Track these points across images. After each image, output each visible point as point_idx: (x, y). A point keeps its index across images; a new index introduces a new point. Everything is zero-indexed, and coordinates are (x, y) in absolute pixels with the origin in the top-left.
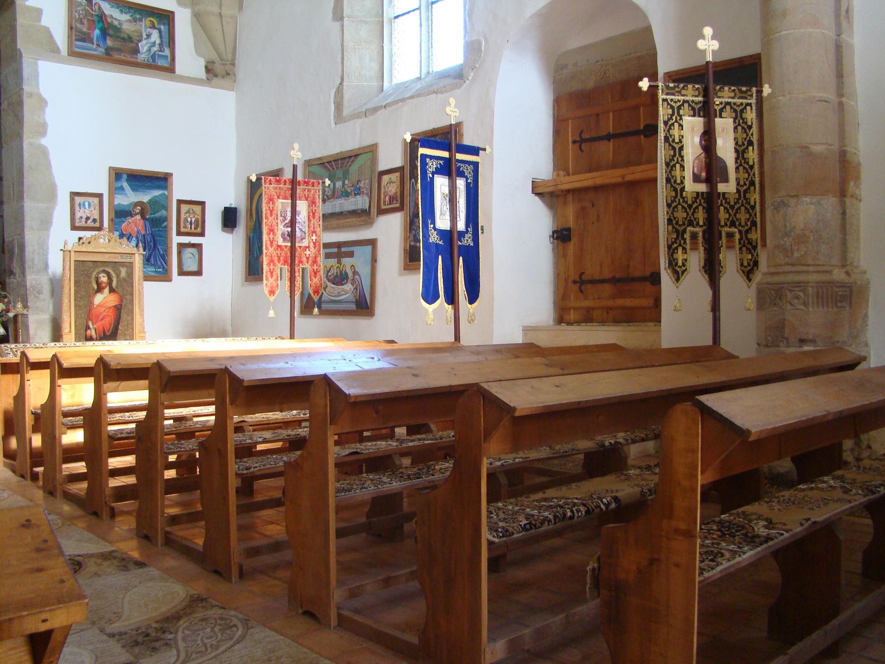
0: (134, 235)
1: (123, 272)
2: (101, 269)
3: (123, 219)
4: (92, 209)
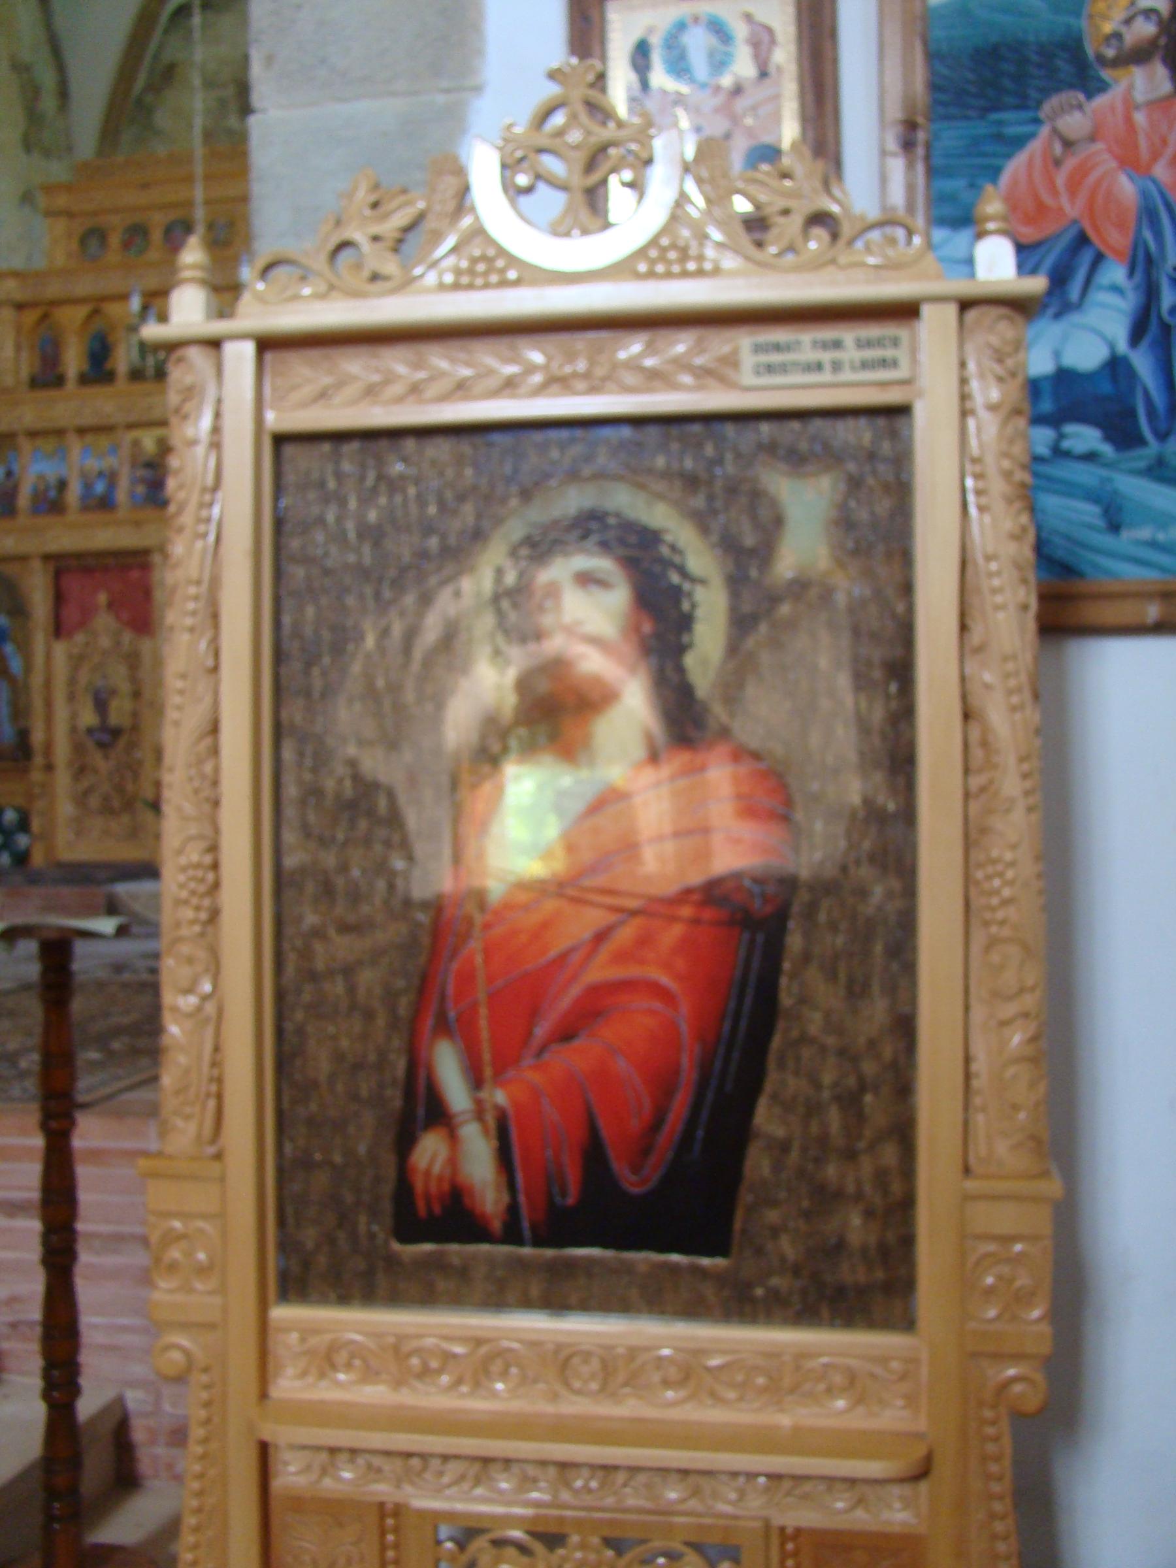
0: (1116, 238)
1: (806, 507)
2: (573, 501)
3: (1012, 121)
4: (743, 66)
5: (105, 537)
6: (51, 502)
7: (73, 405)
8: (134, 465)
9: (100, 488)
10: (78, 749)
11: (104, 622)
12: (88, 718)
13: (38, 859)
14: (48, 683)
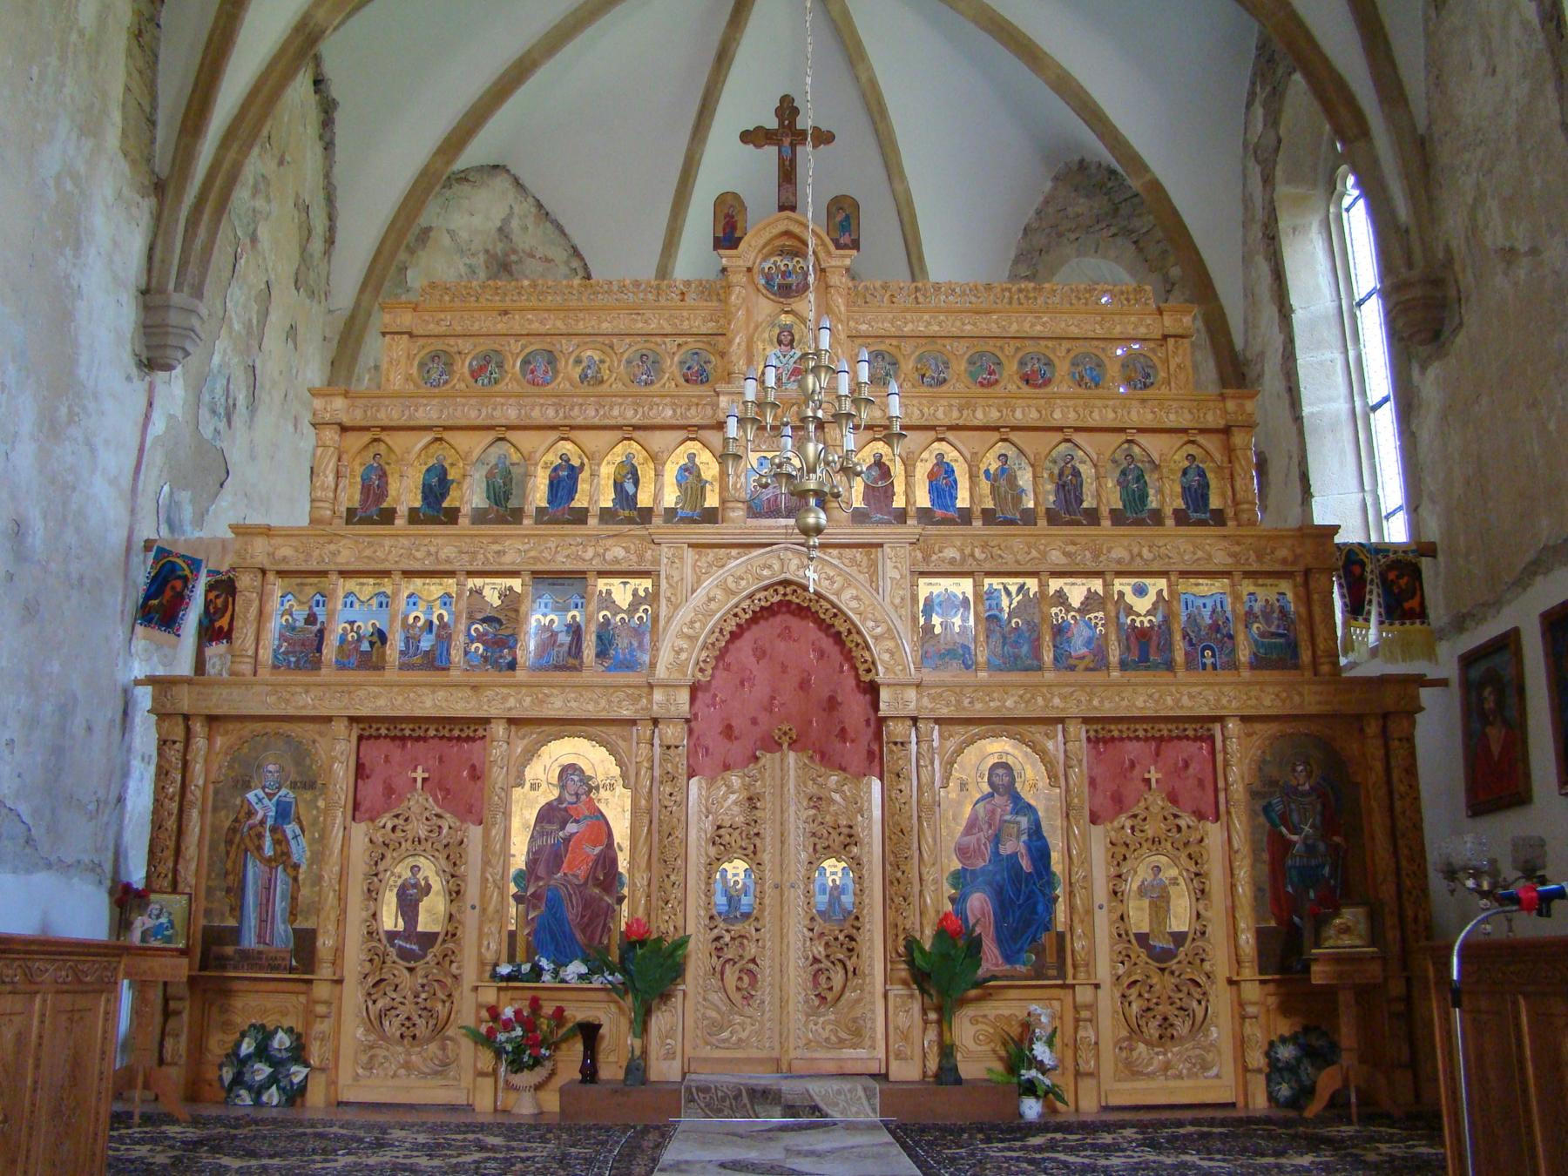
5: (432, 701)
6: (368, 654)
7: (396, 545)
8: (472, 620)
9: (426, 643)
10: (376, 959)
11: (419, 802)
12: (390, 919)
13: (316, 1096)
14: (342, 876)
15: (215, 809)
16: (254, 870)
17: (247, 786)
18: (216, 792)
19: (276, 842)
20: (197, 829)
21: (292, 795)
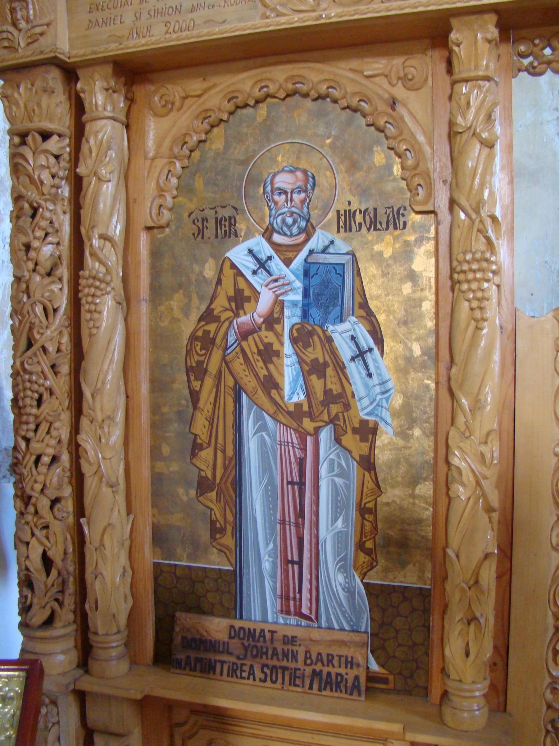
15: (157, 292)
16: (260, 439)
17: (228, 231)
18: (156, 254)
19: (312, 369)
20: (118, 340)
21: (342, 246)
